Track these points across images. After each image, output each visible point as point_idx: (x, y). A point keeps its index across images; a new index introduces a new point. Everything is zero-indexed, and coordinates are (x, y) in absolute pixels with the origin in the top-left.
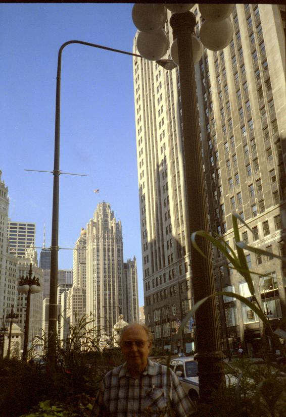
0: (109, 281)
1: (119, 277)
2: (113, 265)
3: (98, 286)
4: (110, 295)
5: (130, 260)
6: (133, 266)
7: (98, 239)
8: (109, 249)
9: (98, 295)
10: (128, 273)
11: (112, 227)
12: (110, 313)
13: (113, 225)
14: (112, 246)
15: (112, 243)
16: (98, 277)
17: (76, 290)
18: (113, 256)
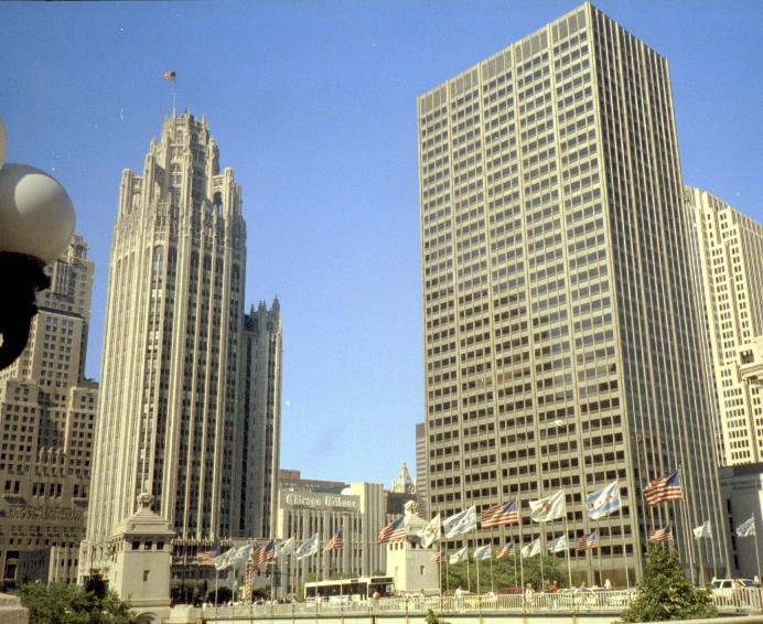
0: (201, 362)
1: (231, 355)
2: (217, 310)
3: (165, 372)
4: (199, 405)
5: (262, 307)
6: (271, 326)
7: (174, 218)
8: (207, 259)
9: (163, 401)
10: (254, 342)
11: (217, 196)
12: (196, 464)
13: (225, 191)
14: (218, 250)
15: (218, 242)
16: (167, 342)
17: (18, 390)
18: (218, 284)
